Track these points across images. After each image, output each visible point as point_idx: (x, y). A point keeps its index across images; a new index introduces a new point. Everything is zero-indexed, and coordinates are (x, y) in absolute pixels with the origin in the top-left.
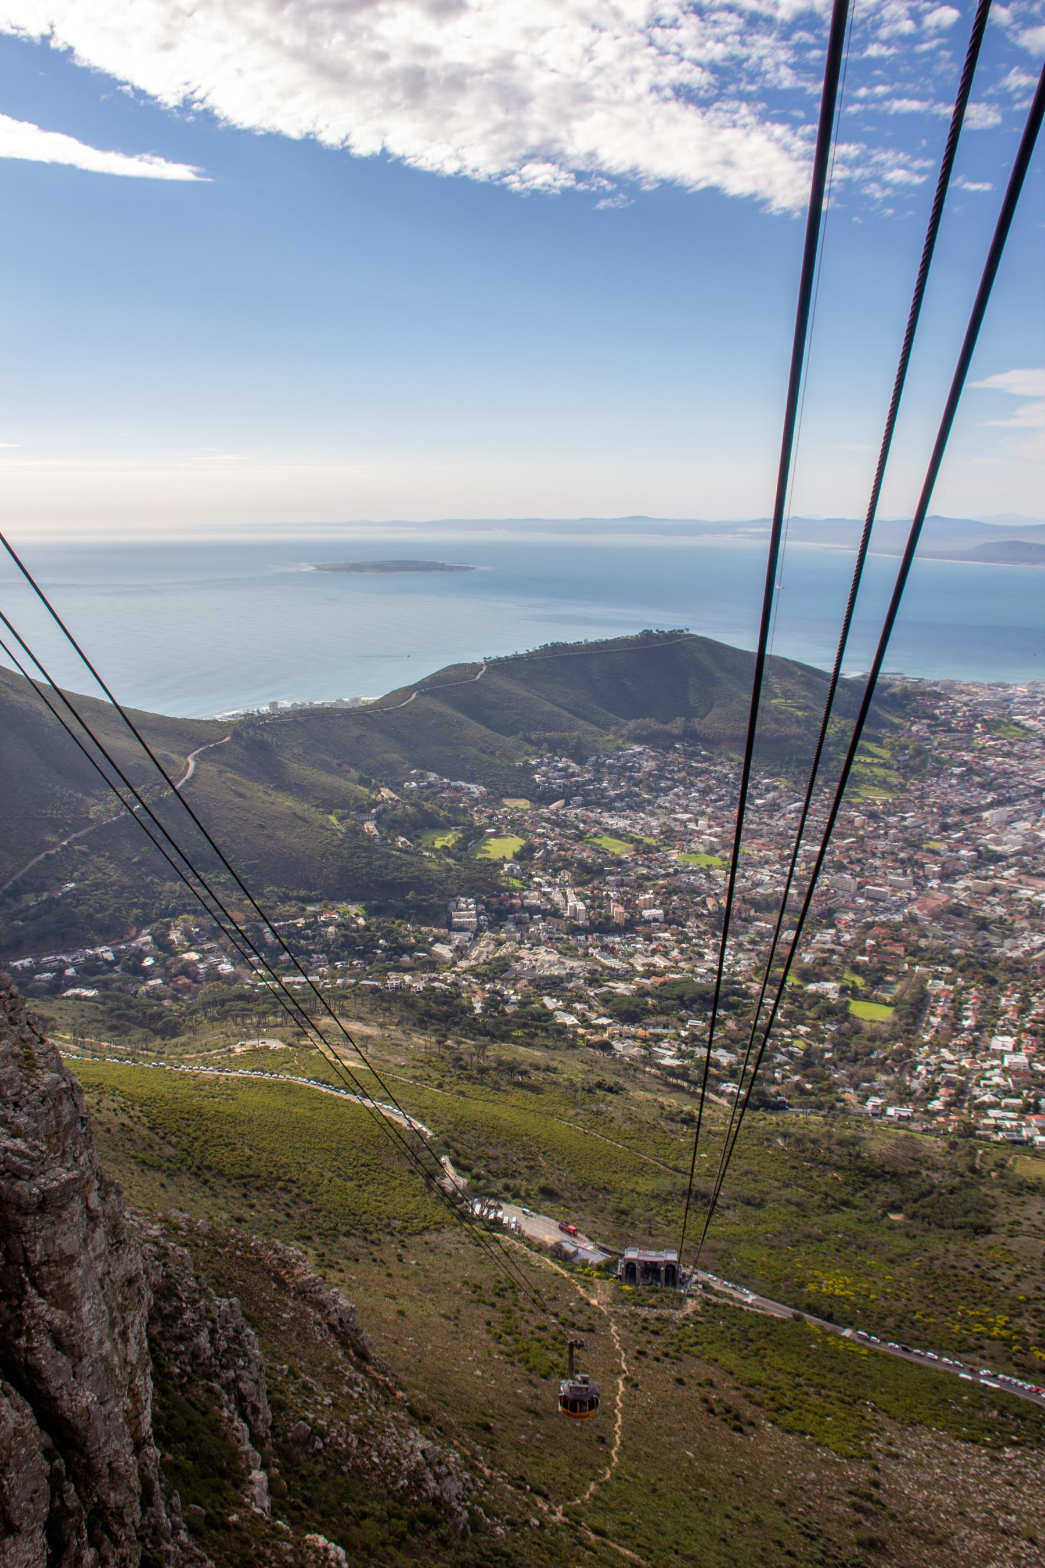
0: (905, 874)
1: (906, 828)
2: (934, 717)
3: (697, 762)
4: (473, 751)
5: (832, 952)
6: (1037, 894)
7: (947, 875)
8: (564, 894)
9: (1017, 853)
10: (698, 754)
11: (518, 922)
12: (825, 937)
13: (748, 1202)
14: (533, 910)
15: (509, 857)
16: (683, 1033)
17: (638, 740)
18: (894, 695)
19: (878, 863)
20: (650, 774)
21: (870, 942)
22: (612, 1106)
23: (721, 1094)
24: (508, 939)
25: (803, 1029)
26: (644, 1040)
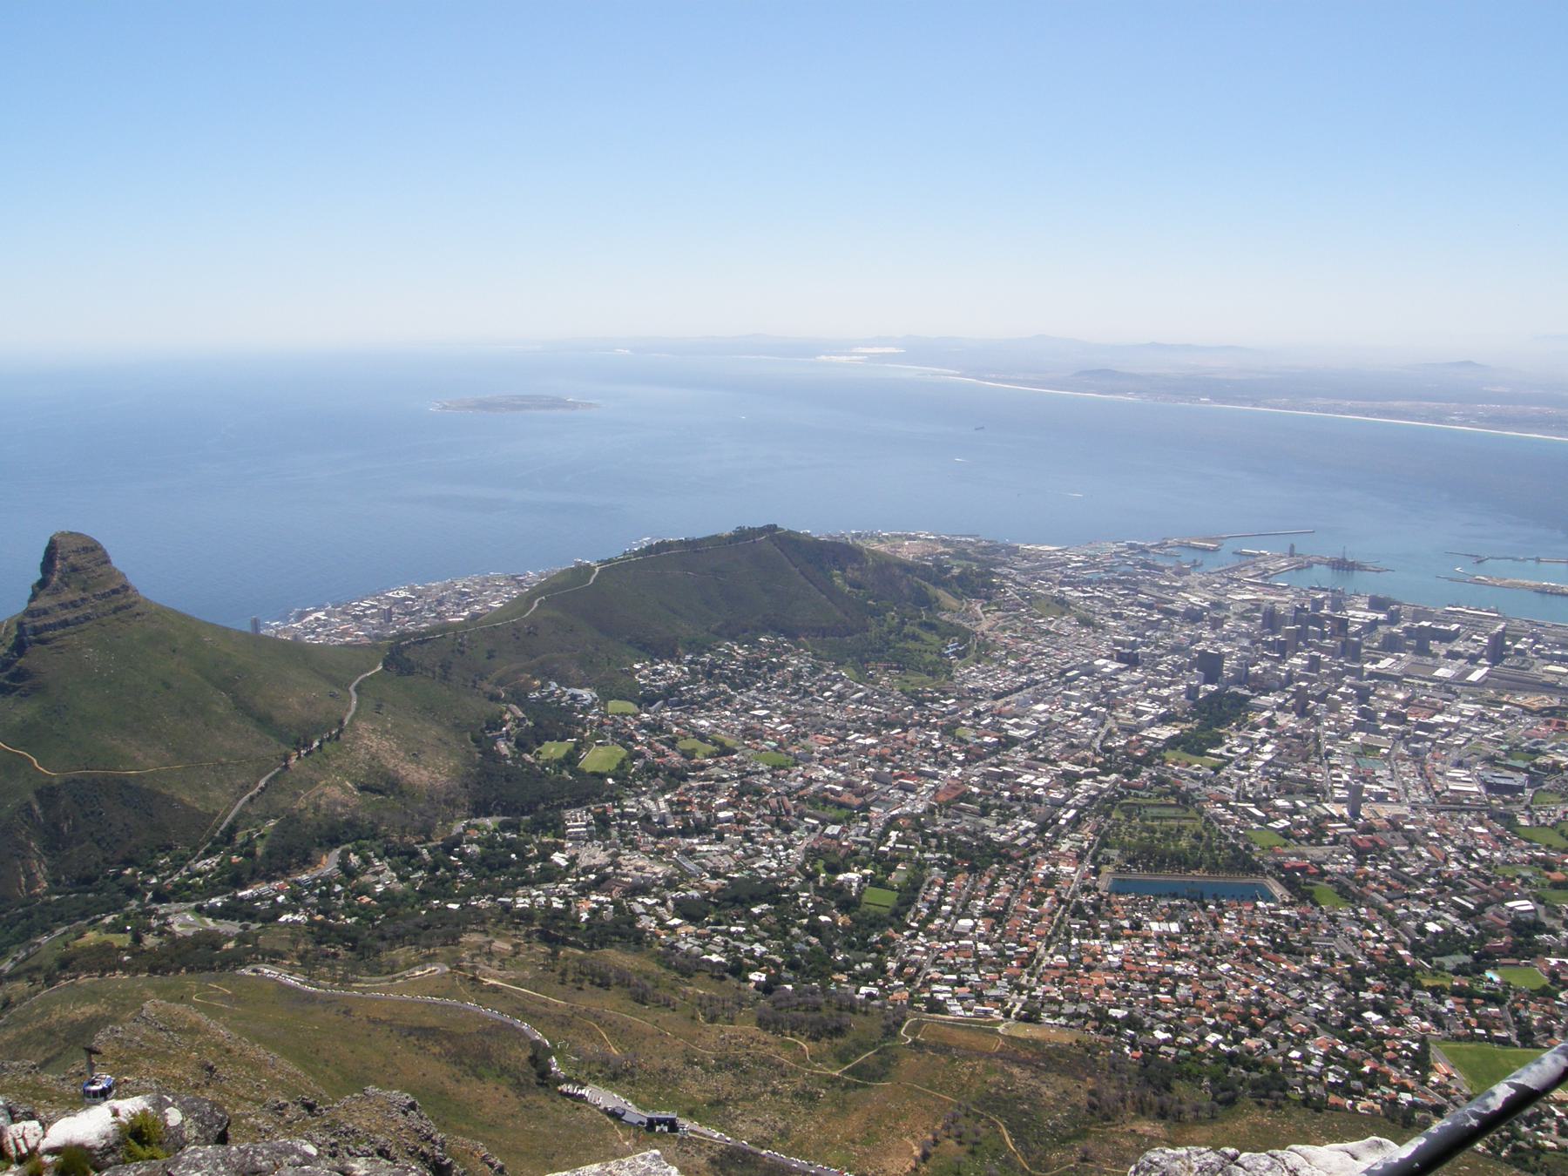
9: (1030, 738)
14: (632, 816)
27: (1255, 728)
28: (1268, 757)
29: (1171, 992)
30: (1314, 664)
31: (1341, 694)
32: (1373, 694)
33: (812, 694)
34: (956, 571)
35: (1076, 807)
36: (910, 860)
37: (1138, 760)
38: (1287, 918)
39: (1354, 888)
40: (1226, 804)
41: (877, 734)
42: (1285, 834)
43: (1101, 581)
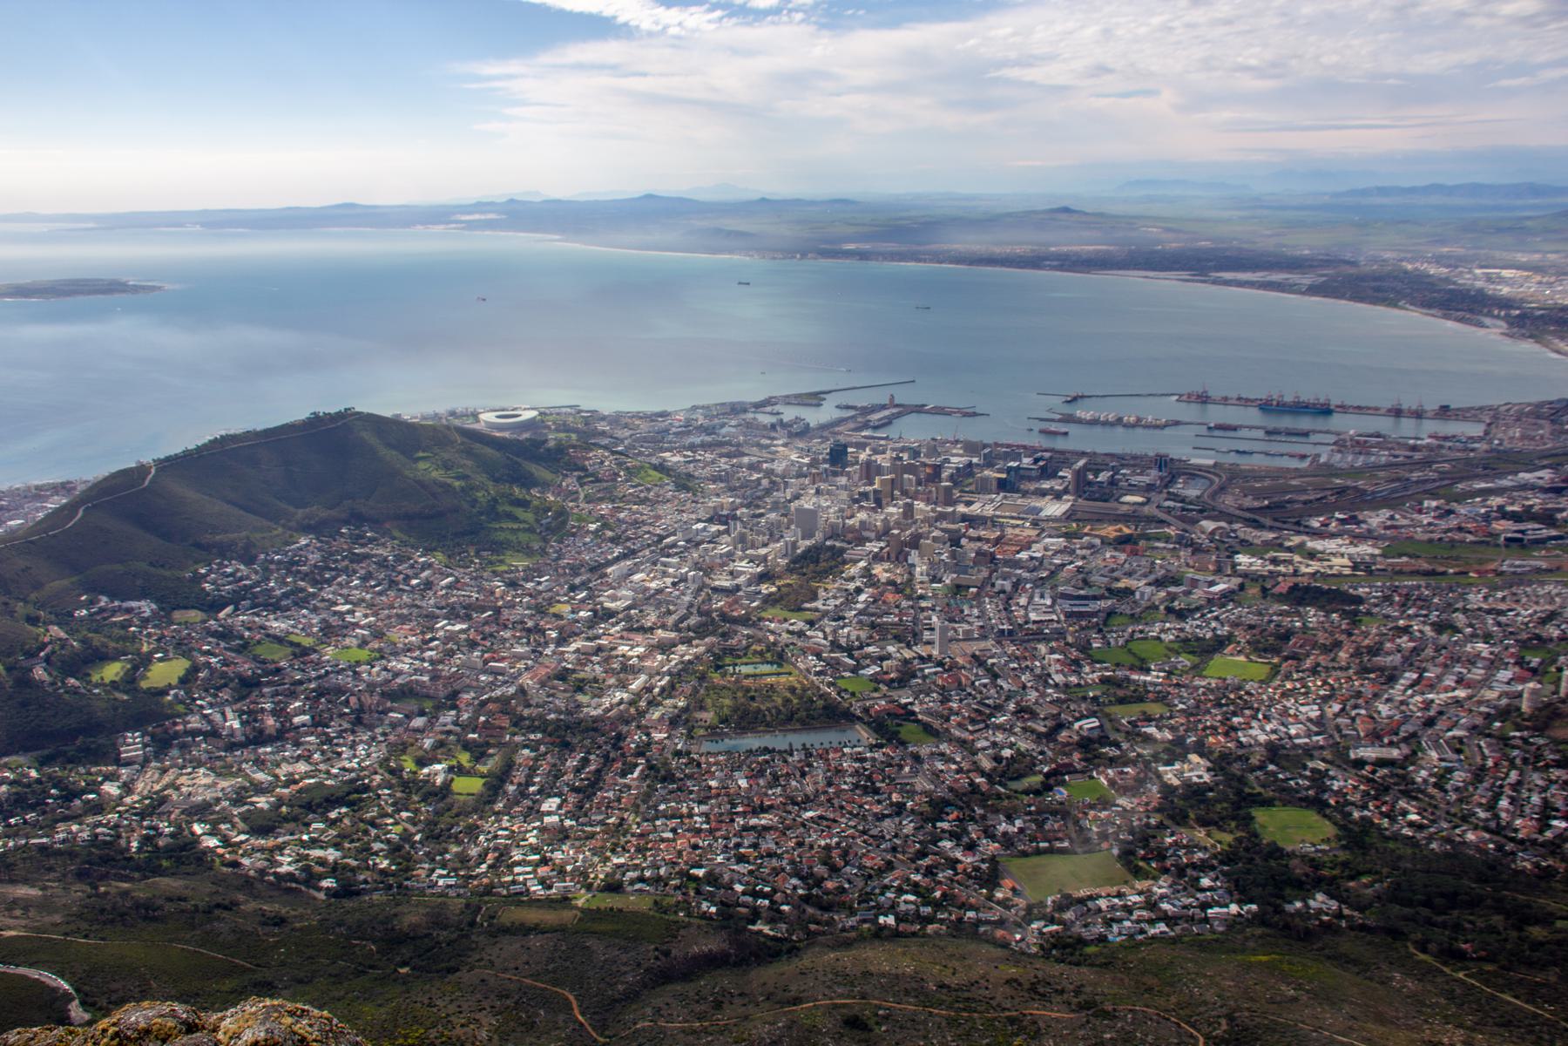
0: (528, 643)
1: (541, 592)
2: (584, 469)
3: (363, 545)
4: (143, 566)
5: (449, 732)
6: (632, 647)
7: (562, 640)
8: (223, 714)
10: (363, 537)
11: (184, 747)
12: (448, 717)
13: (300, 982)
14: (195, 733)
15: (174, 682)
16: (305, 837)
17: (306, 529)
18: (549, 450)
19: (507, 634)
20: (315, 566)
21: (482, 719)
22: (224, 925)
23: (320, 889)
24: (171, 767)
25: (404, 814)
26: (272, 851)
27: (852, 579)
28: (859, 606)
29: (755, 846)
30: (909, 511)
31: (935, 539)
32: (964, 535)
33: (397, 583)
34: (551, 444)
35: (669, 673)
36: (500, 745)
37: (735, 621)
38: (874, 759)
39: (936, 723)
40: (818, 655)
41: (468, 618)
42: (875, 679)
43: (705, 446)
